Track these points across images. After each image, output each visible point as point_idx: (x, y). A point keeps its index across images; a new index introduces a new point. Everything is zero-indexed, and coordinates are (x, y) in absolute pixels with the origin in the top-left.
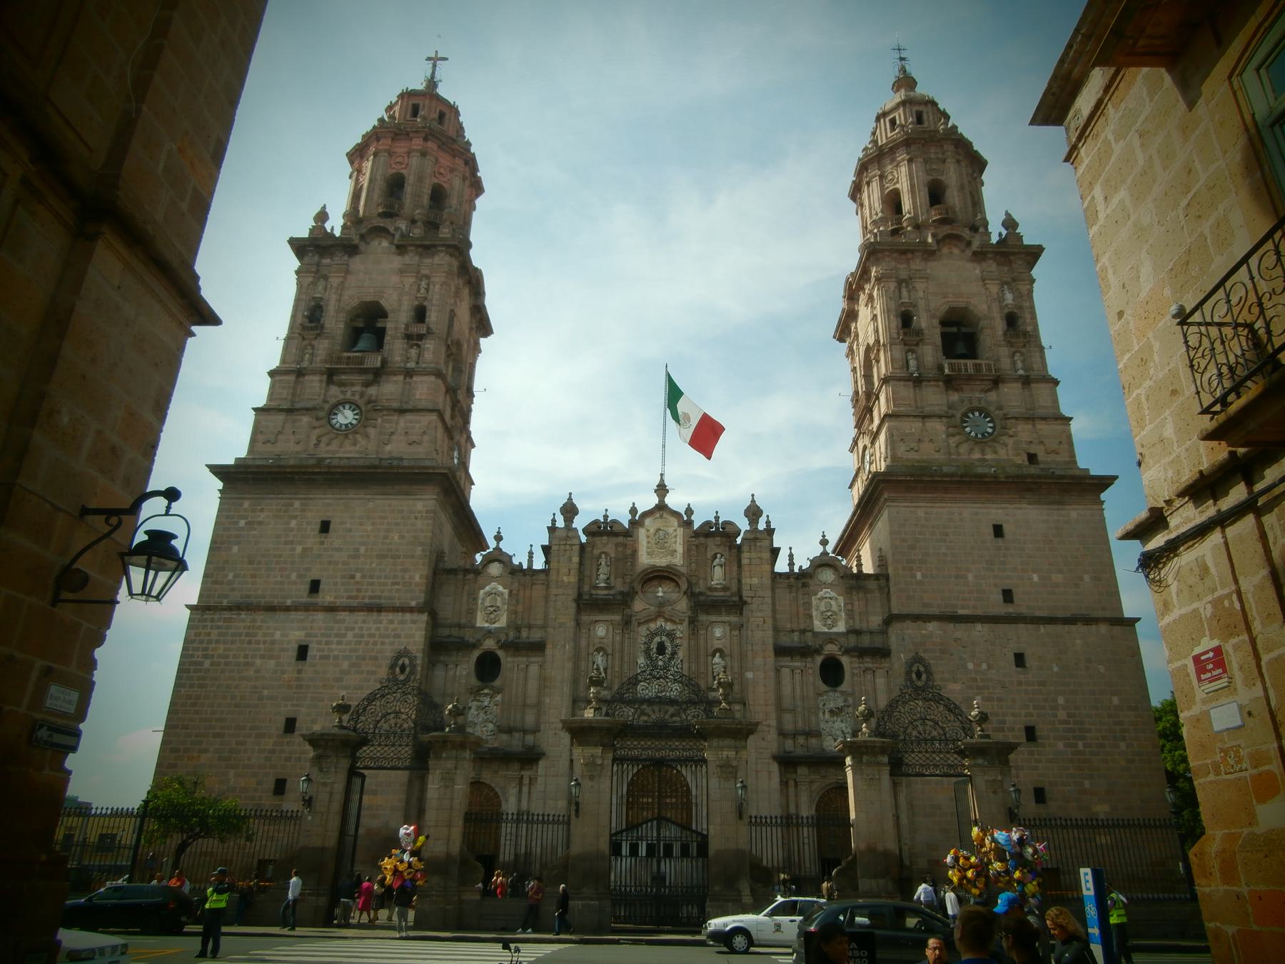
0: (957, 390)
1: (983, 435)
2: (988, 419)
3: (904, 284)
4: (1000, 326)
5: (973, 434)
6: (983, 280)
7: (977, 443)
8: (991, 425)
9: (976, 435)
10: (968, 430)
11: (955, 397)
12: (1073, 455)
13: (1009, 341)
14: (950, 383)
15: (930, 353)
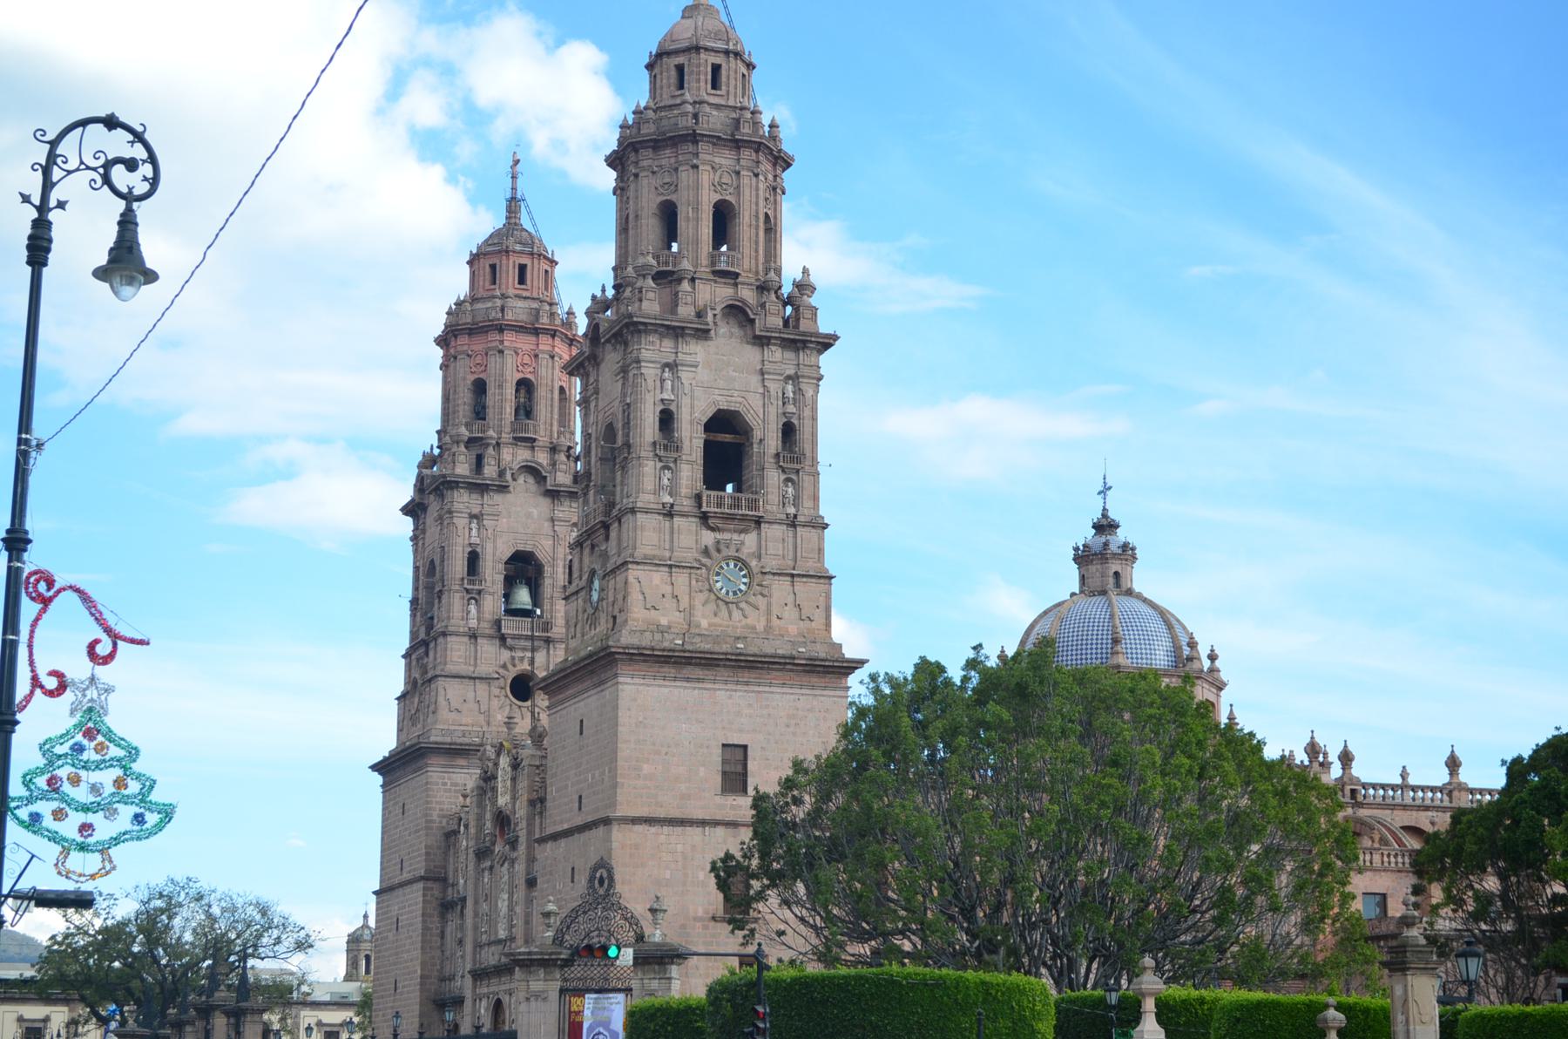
0: (713, 529)
1: (735, 593)
2: (743, 573)
3: (667, 369)
4: (773, 443)
5: (724, 591)
6: (762, 373)
7: (727, 603)
8: (745, 580)
9: (727, 593)
10: (719, 585)
11: (708, 538)
12: (828, 625)
13: (781, 466)
14: (704, 518)
15: (690, 473)
